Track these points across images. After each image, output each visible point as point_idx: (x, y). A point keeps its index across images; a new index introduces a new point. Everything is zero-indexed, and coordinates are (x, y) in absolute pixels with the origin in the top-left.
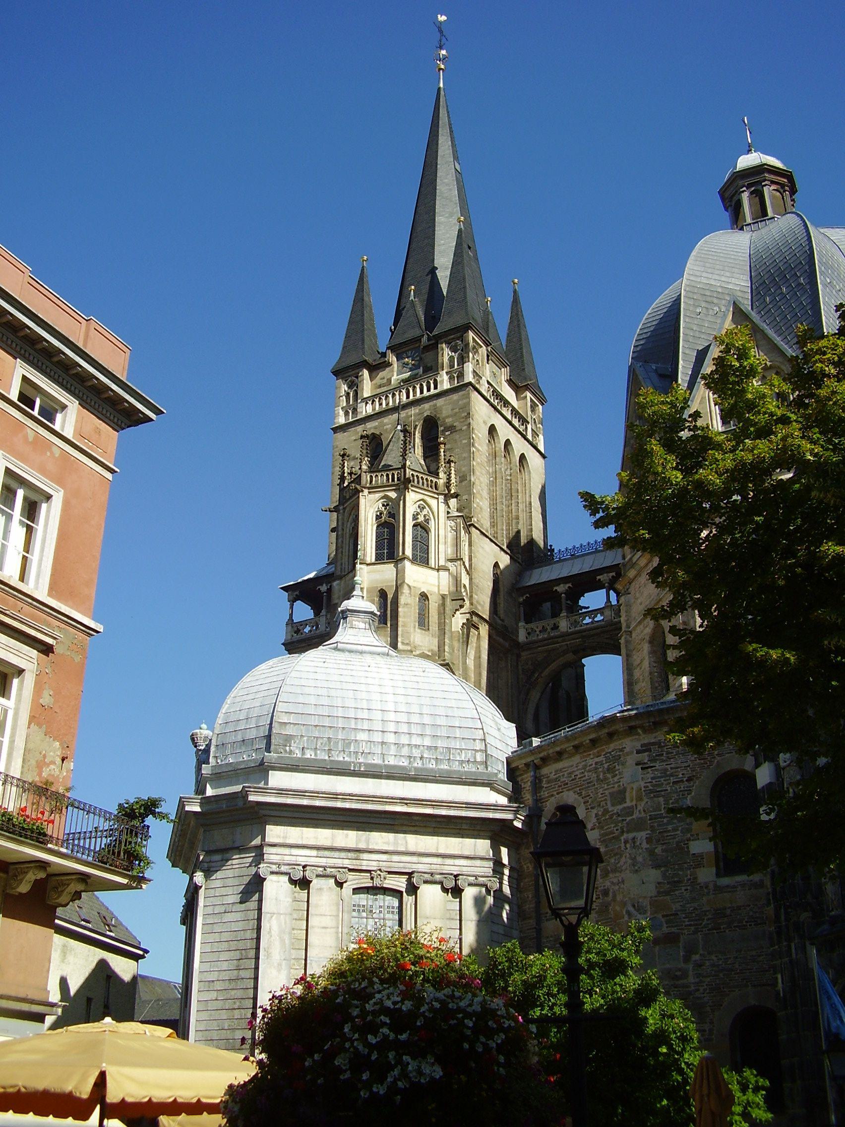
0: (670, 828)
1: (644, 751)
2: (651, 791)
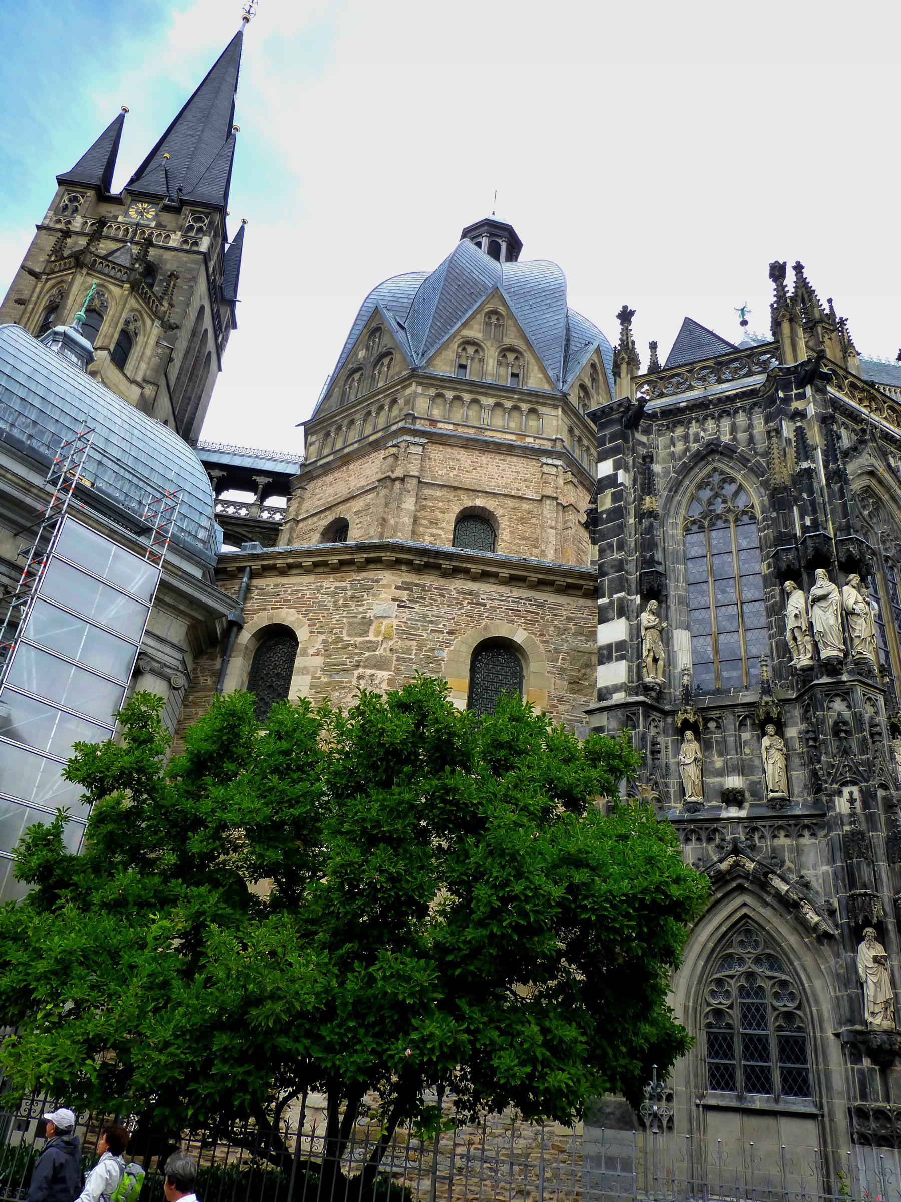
1: (405, 589)
2: (404, 632)
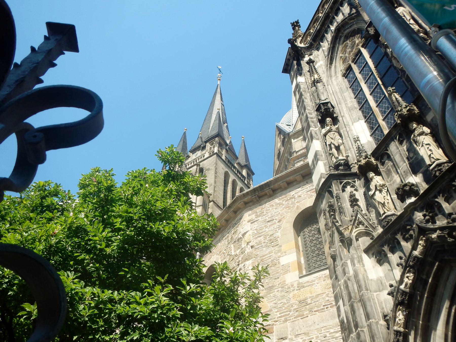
2: (256, 234)
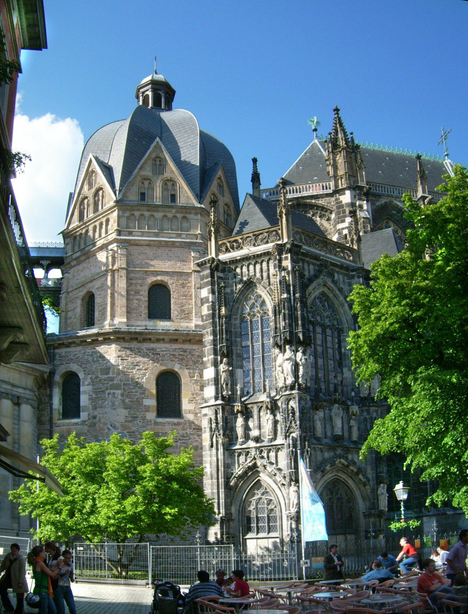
0: (134, 391)
